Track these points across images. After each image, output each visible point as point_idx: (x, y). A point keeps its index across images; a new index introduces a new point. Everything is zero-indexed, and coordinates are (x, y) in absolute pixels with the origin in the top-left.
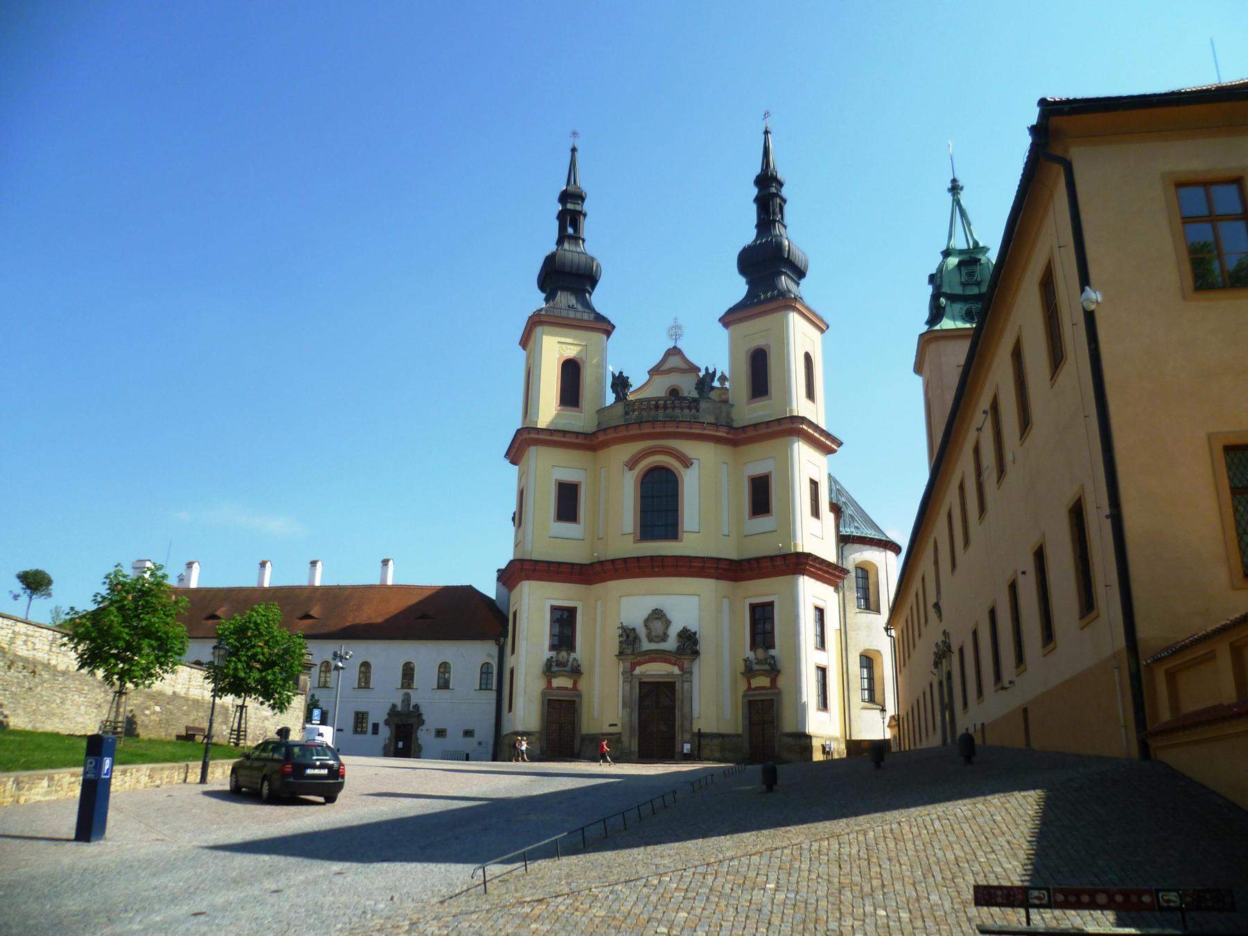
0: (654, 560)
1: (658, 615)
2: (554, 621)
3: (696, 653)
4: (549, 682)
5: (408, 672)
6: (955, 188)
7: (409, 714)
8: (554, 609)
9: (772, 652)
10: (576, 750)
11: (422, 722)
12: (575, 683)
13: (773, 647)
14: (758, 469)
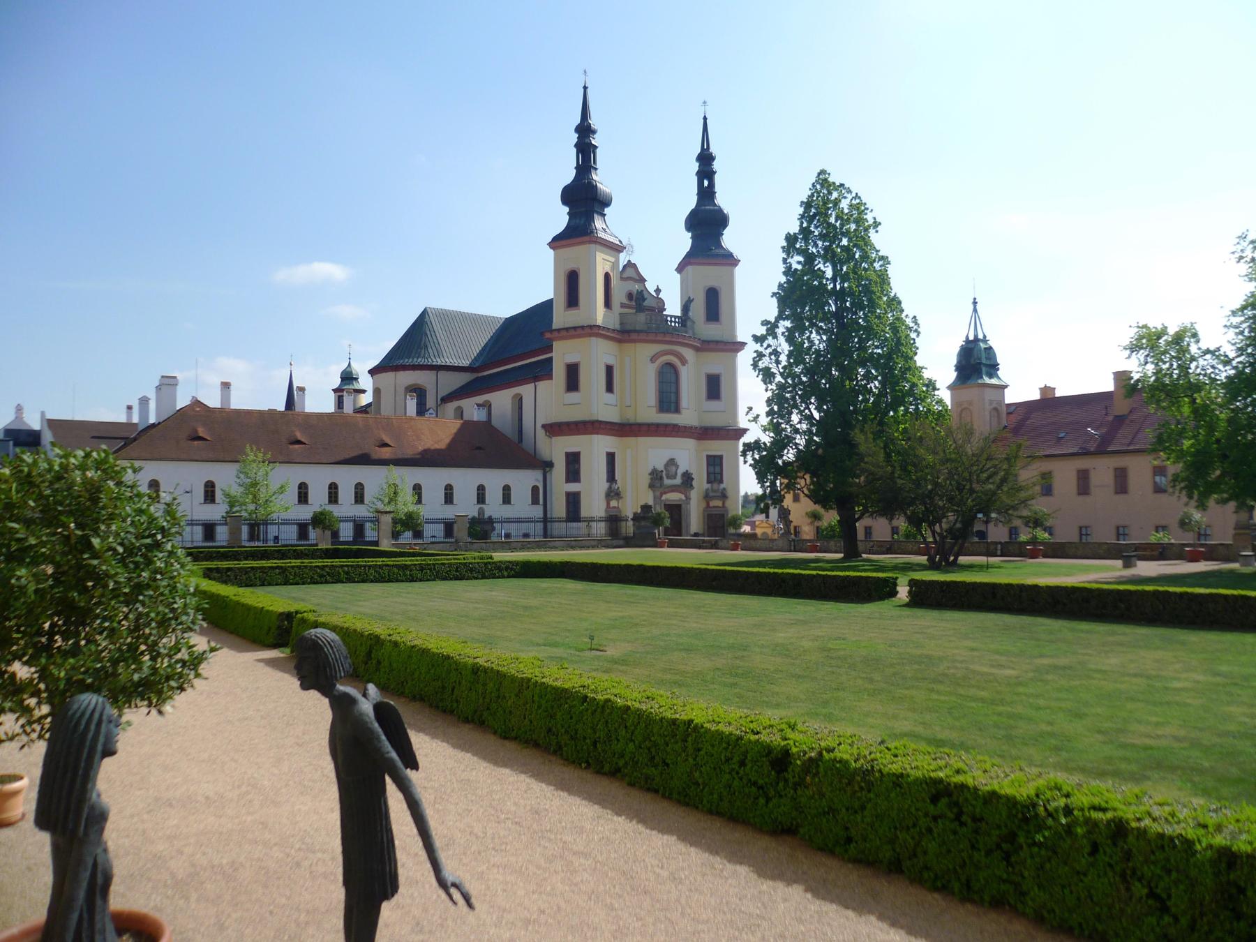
0: (666, 425)
1: (672, 462)
5: (481, 491)
6: (975, 303)
9: (722, 486)
13: (721, 481)
14: (714, 370)
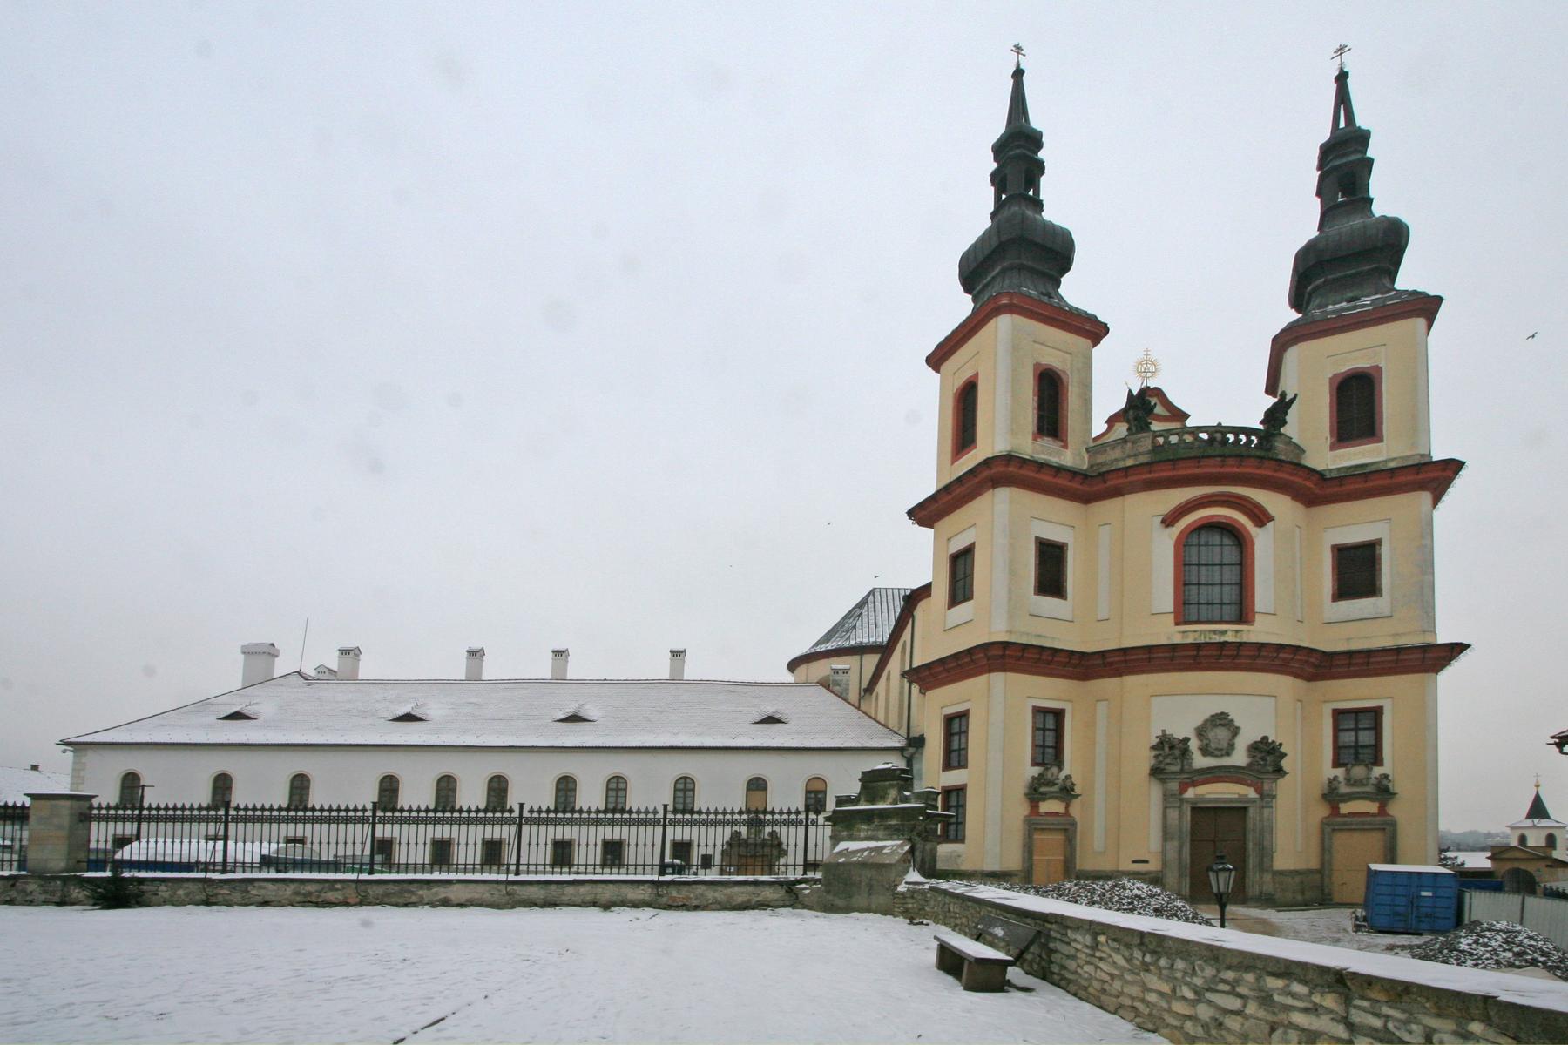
1: (1221, 720)
3: (1279, 771)
9: (1377, 771)
13: (1377, 760)
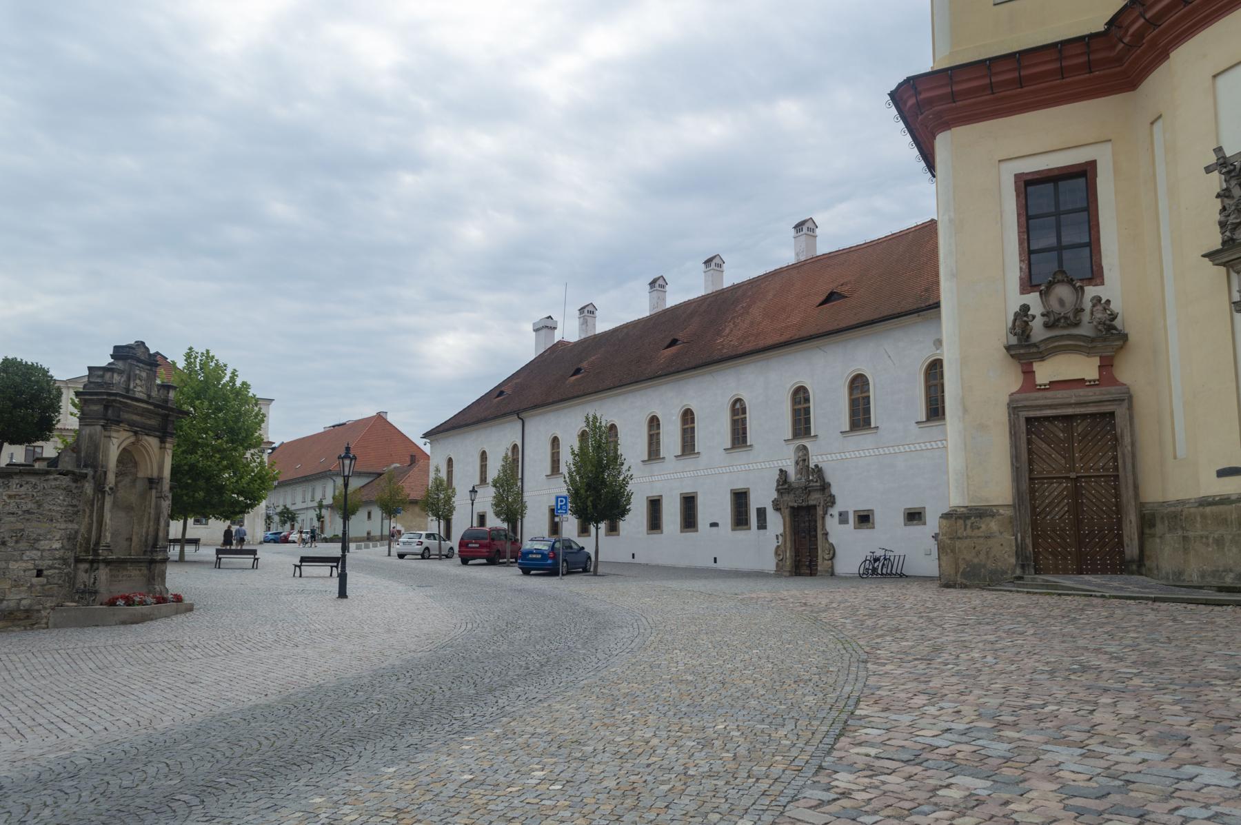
2: (1028, 220)
4: (1028, 373)
7: (807, 490)
8: (1027, 184)
10: (1132, 550)
11: (832, 501)
12: (1107, 365)
